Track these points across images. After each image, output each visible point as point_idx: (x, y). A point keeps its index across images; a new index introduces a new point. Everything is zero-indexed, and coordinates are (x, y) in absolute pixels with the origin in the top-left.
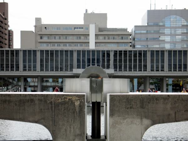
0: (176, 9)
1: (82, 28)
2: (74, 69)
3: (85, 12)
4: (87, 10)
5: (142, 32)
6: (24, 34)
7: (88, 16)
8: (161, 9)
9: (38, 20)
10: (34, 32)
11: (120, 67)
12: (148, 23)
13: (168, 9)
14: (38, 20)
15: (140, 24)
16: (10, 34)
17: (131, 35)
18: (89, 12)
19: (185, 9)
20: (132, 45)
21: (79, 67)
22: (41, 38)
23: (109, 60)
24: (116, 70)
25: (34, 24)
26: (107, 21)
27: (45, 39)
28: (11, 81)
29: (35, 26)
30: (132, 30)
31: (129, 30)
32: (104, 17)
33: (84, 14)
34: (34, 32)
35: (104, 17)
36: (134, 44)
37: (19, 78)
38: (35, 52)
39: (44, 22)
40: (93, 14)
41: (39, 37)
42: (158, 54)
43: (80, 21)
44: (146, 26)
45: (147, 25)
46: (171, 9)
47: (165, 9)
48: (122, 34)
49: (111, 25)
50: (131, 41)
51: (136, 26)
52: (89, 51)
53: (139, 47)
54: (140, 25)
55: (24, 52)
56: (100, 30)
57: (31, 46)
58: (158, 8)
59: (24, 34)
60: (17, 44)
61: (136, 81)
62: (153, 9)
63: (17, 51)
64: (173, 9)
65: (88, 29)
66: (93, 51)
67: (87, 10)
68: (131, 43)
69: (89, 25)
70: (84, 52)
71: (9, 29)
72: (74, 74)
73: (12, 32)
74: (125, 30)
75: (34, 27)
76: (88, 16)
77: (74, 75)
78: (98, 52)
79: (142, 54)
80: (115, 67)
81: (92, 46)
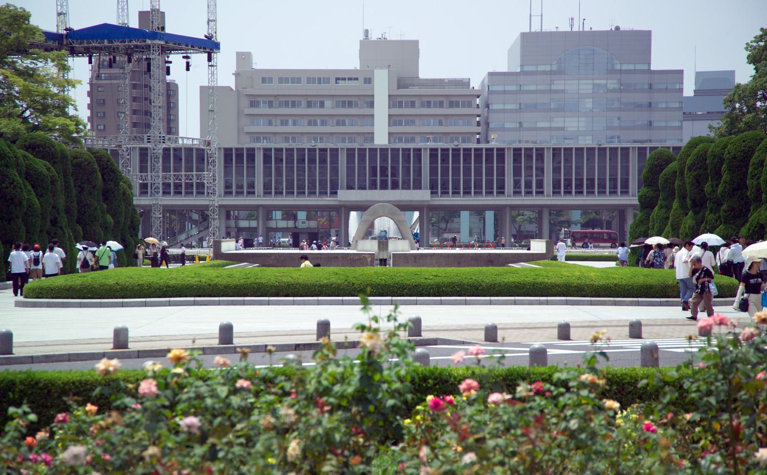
0: (593, 29)
1: (357, 79)
2: (339, 191)
3: (362, 37)
4: (367, 32)
5: (508, 88)
8: (555, 30)
10: (234, 89)
12: (522, 66)
13: (575, 29)
15: (504, 68)
17: (478, 96)
18: (374, 36)
19: (617, 28)
20: (482, 123)
25: (233, 69)
26: (420, 60)
27: (263, 110)
29: (237, 75)
30: (483, 82)
31: (476, 84)
32: (411, 49)
33: (361, 41)
34: (234, 89)
35: (411, 49)
36: (487, 118)
39: (260, 63)
41: (246, 102)
44: (516, 74)
45: (519, 70)
46: (581, 30)
49: (426, 71)
50: (478, 111)
51: (491, 74)
54: (507, 71)
56: (402, 83)
58: (549, 27)
61: (490, 216)
62: (536, 28)
64: (587, 29)
65: (369, 81)
67: (367, 32)
68: (479, 116)
69: (373, 71)
70: (362, 151)
72: (340, 201)
73: (177, 85)
74: (465, 83)
75: (234, 76)
77: (341, 203)
78: (395, 151)
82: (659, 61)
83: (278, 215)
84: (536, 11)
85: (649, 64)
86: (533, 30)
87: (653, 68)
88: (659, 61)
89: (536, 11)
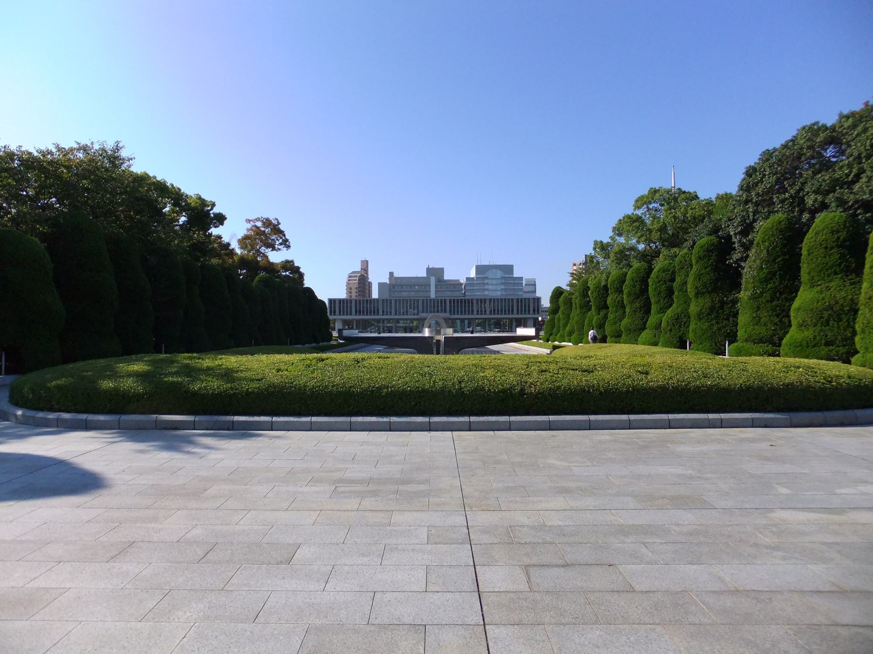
6: (381, 285)
7: (430, 271)
9: (391, 274)
13: (491, 264)
14: (391, 274)
16: (370, 283)
18: (430, 267)
21: (423, 312)
24: (451, 314)
25: (388, 277)
28: (373, 322)
29: (390, 279)
32: (441, 270)
35: (441, 270)
37: (378, 321)
39: (396, 275)
40: (433, 269)
42: (482, 301)
47: (488, 264)
48: (456, 284)
49: (447, 277)
52: (431, 300)
53: (469, 295)
55: (383, 300)
57: (386, 296)
59: (381, 285)
60: (375, 295)
61: (466, 322)
62: (479, 264)
63: (377, 300)
66: (434, 300)
71: (369, 280)
76: (430, 271)
79: (470, 302)
80: (450, 311)
81: (433, 295)
82: (516, 275)
85: (513, 274)
86: (479, 264)
87: (514, 276)
88: (516, 275)
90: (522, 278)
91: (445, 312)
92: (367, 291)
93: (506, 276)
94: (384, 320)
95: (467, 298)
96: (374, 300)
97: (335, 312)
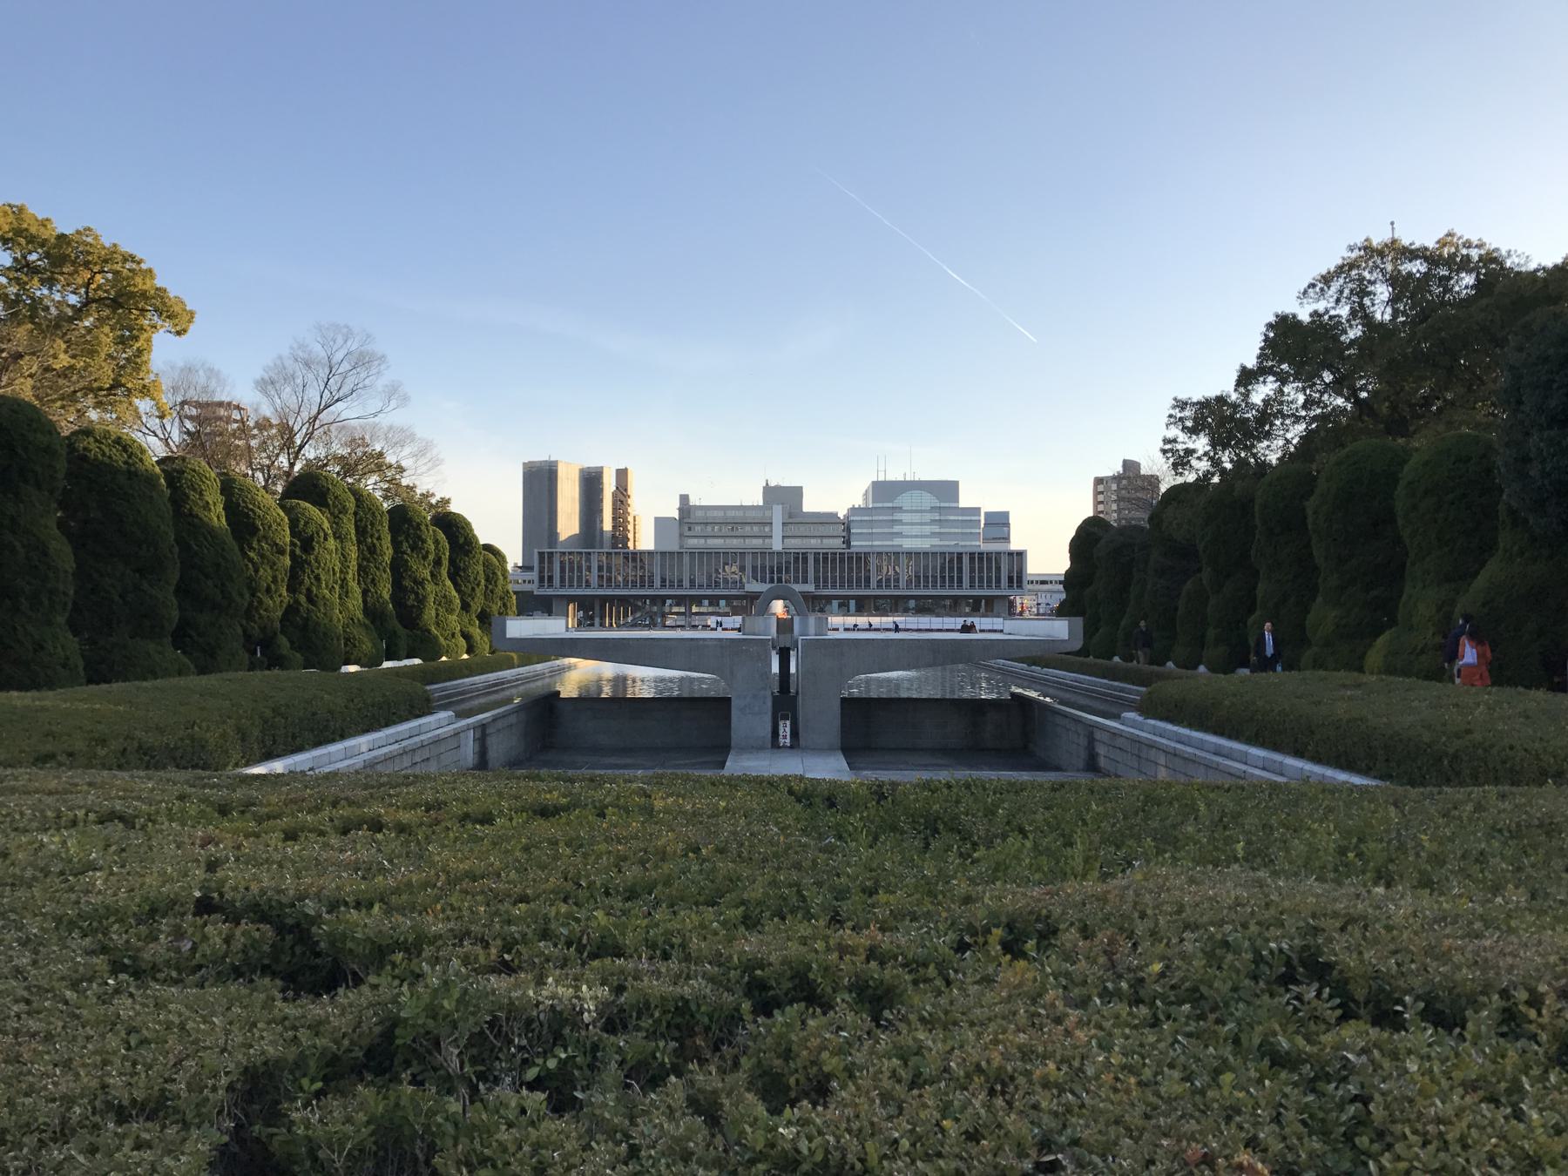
6: (660, 522)
7: (771, 492)
9: (684, 499)
11: (825, 581)
13: (908, 479)
14: (684, 499)
18: (772, 484)
22: (690, 529)
23: (805, 571)
24: (817, 587)
25: (678, 505)
29: (680, 509)
31: (841, 515)
32: (797, 492)
35: (797, 492)
37: (654, 599)
38: (680, 554)
39: (694, 501)
40: (778, 488)
43: (758, 500)
48: (827, 519)
49: (808, 506)
55: (663, 554)
58: (890, 477)
59: (660, 522)
62: (881, 478)
63: (650, 553)
66: (779, 553)
74: (835, 515)
76: (771, 492)
79: (862, 558)
80: (817, 580)
81: (777, 545)
82: (965, 502)
83: (706, 602)
84: (881, 468)
88: (965, 502)
89: (881, 468)
90: (979, 509)
91: (805, 581)
92: (630, 536)
93: (943, 505)
94: (663, 599)
95: (852, 550)
96: (642, 553)
97: (550, 578)
